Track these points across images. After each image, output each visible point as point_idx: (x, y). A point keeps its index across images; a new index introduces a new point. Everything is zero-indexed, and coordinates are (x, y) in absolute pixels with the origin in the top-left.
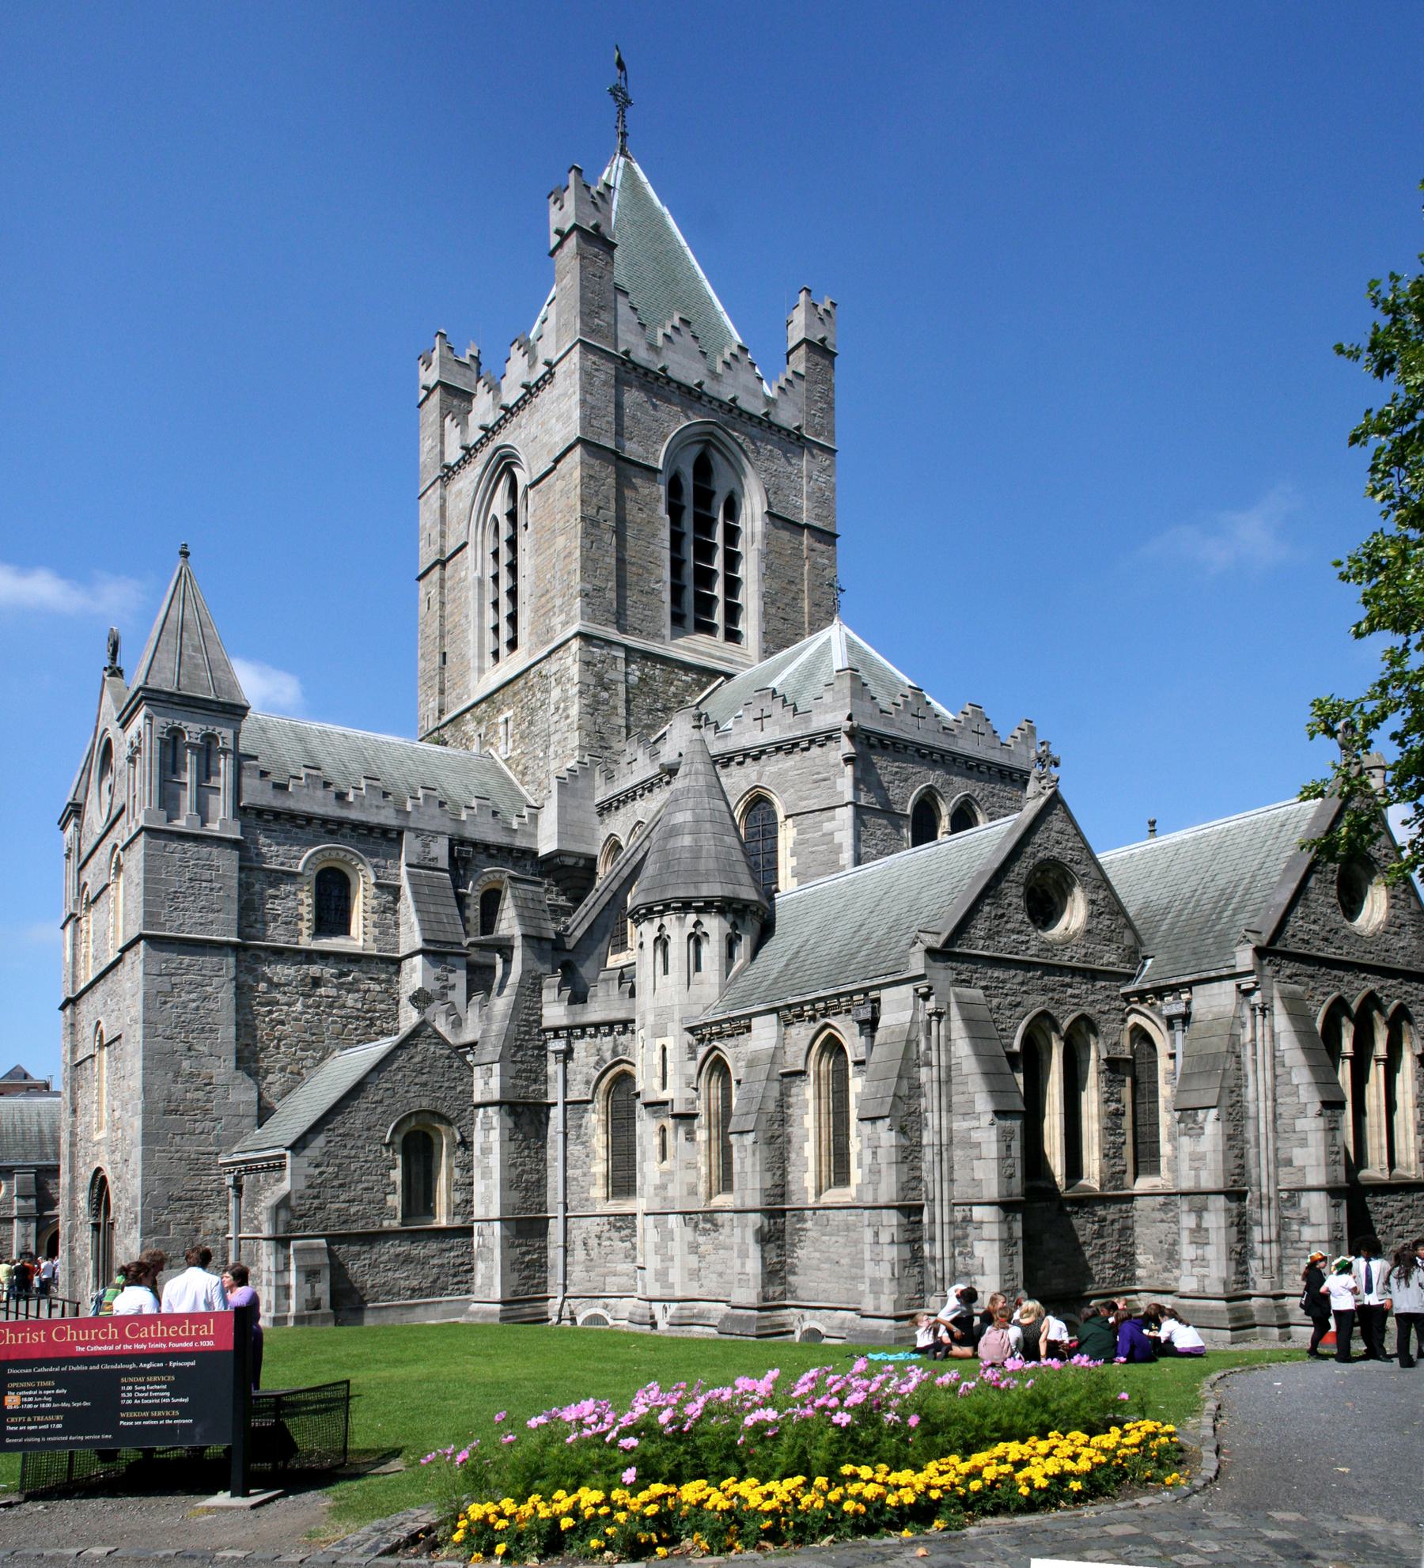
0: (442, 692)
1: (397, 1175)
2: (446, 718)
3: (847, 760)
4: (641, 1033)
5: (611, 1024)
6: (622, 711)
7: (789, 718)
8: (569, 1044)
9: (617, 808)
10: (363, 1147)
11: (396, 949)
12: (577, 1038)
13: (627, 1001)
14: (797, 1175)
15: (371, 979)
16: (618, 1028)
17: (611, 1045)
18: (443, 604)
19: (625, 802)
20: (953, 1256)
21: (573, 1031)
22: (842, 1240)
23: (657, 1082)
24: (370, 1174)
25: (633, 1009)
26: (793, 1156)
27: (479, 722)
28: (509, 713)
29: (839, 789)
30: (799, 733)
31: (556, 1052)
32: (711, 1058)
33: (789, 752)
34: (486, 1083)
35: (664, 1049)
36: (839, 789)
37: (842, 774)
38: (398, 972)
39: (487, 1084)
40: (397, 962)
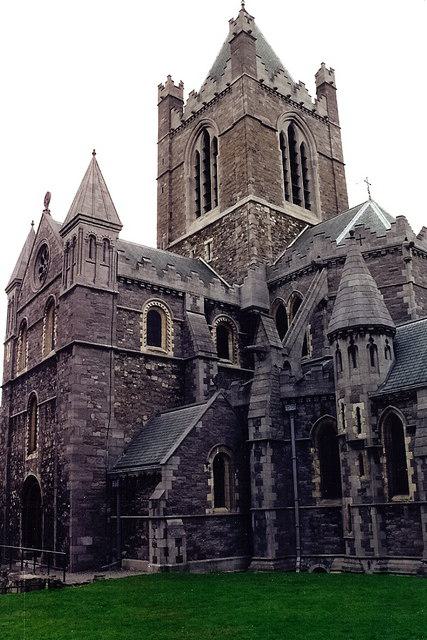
0: (170, 230)
5: (320, 396)
6: (270, 238)
13: (329, 385)
23: (355, 429)
27: (193, 244)
33: (375, 257)
34: (257, 429)
35: (358, 409)
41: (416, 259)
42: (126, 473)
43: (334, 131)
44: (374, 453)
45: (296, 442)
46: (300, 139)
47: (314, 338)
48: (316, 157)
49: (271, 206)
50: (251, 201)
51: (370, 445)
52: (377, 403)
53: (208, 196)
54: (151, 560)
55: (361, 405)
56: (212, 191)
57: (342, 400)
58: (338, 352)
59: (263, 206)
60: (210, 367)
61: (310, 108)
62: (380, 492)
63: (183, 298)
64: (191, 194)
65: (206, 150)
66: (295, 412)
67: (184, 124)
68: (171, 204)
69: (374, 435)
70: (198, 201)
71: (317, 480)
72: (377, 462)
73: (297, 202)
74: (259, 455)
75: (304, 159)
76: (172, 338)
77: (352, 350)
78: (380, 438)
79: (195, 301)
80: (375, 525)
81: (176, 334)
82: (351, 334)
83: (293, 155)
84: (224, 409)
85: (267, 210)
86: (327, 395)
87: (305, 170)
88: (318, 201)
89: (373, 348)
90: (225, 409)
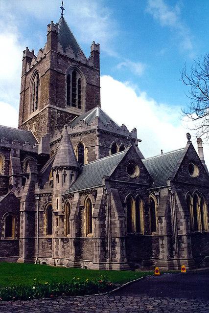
0: (23, 117)
1: (4, 227)
5: (48, 194)
7: (86, 127)
16: (49, 194)
18: (24, 99)
20: (112, 250)
23: (56, 207)
25: (52, 191)
28: (35, 123)
39: (23, 207)
40: (9, 177)
44: (62, 217)
46: (78, 77)
49: (59, 108)
55: (59, 198)
59: (54, 109)
61: (84, 63)
62: (63, 233)
64: (31, 101)
65: (38, 82)
67: (31, 70)
68: (24, 106)
70: (34, 105)
71: (45, 227)
72: (63, 221)
73: (74, 106)
77: (58, 176)
79: (15, 152)
80: (60, 246)
82: (57, 169)
83: (74, 85)
86: (51, 193)
88: (83, 105)
89: (65, 175)
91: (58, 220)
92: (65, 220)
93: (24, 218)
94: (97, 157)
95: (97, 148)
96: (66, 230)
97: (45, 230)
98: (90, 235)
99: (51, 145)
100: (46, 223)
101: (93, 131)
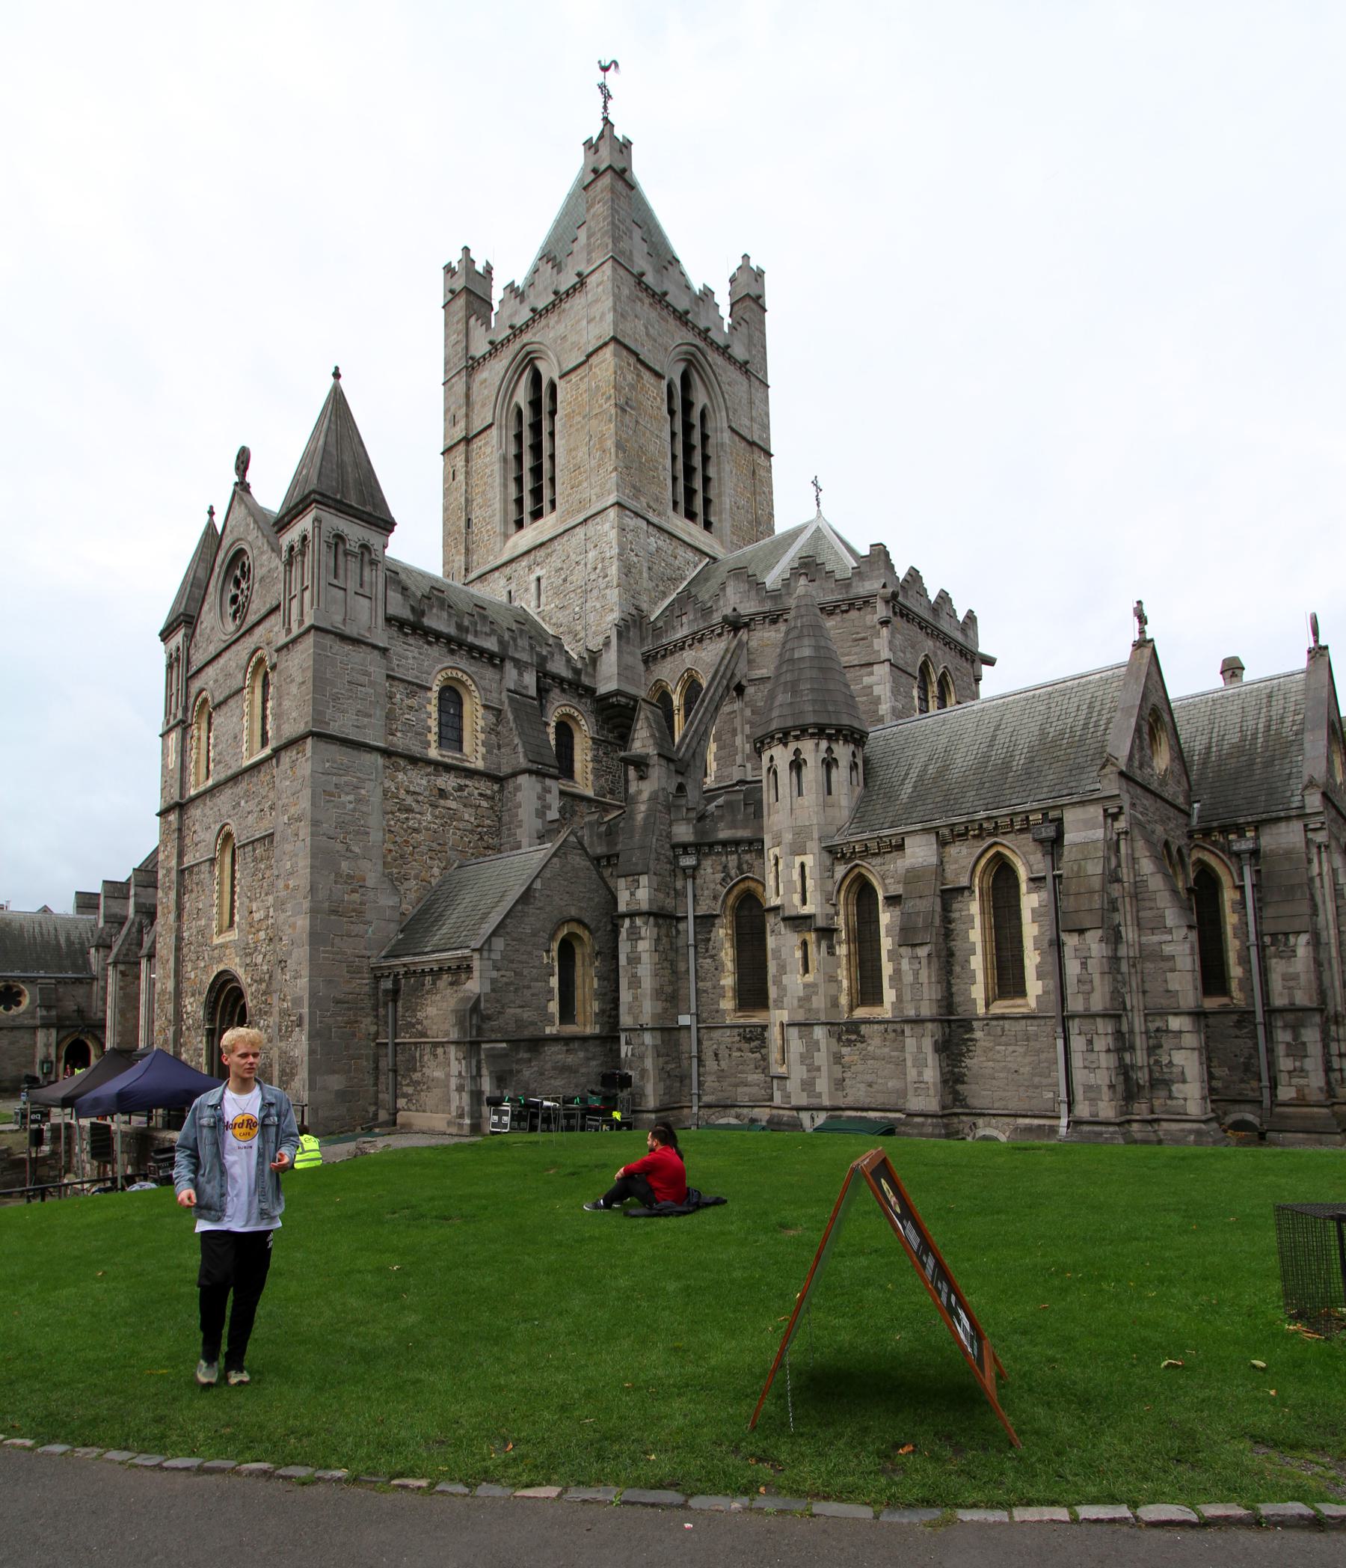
2: (472, 576)
3: (885, 623)
4: (771, 853)
5: (737, 843)
6: (645, 575)
8: (699, 861)
9: (664, 657)
10: (530, 953)
11: (499, 768)
12: (707, 855)
14: (962, 986)
15: (481, 795)
17: (735, 863)
19: (672, 653)
21: (703, 847)
22: (1020, 1050)
23: (797, 898)
24: (537, 980)
26: (957, 969)
29: (876, 648)
30: (840, 597)
31: (684, 869)
32: (852, 876)
33: (831, 613)
34: (632, 894)
35: (803, 866)
36: (876, 648)
37: (878, 635)
38: (501, 790)
41: (897, 621)
42: (404, 965)
43: (757, 396)
44: (827, 933)
45: (696, 917)
46: (700, 398)
47: (719, 748)
48: (727, 436)
50: (618, 504)
51: (820, 922)
52: (834, 853)
53: (537, 493)
54: (454, 1114)
56: (546, 482)
57: (777, 851)
58: (773, 771)
59: (637, 514)
60: (547, 790)
63: (500, 668)
64: (505, 486)
65: (536, 404)
66: (695, 868)
69: (831, 911)
70: (519, 502)
71: (728, 981)
73: (690, 515)
74: (635, 936)
75: (705, 438)
76: (481, 736)
77: (797, 765)
78: (837, 914)
81: (490, 731)
84: (578, 860)
85: (644, 524)
87: (706, 459)
89: (829, 763)
90: (578, 858)
91: (812, 949)
92: (842, 950)
93: (643, 946)
94: (884, 708)
95: (882, 671)
96: (850, 988)
97: (730, 994)
98: (999, 1008)
99: (649, 659)
100: (730, 965)
101: (867, 602)
